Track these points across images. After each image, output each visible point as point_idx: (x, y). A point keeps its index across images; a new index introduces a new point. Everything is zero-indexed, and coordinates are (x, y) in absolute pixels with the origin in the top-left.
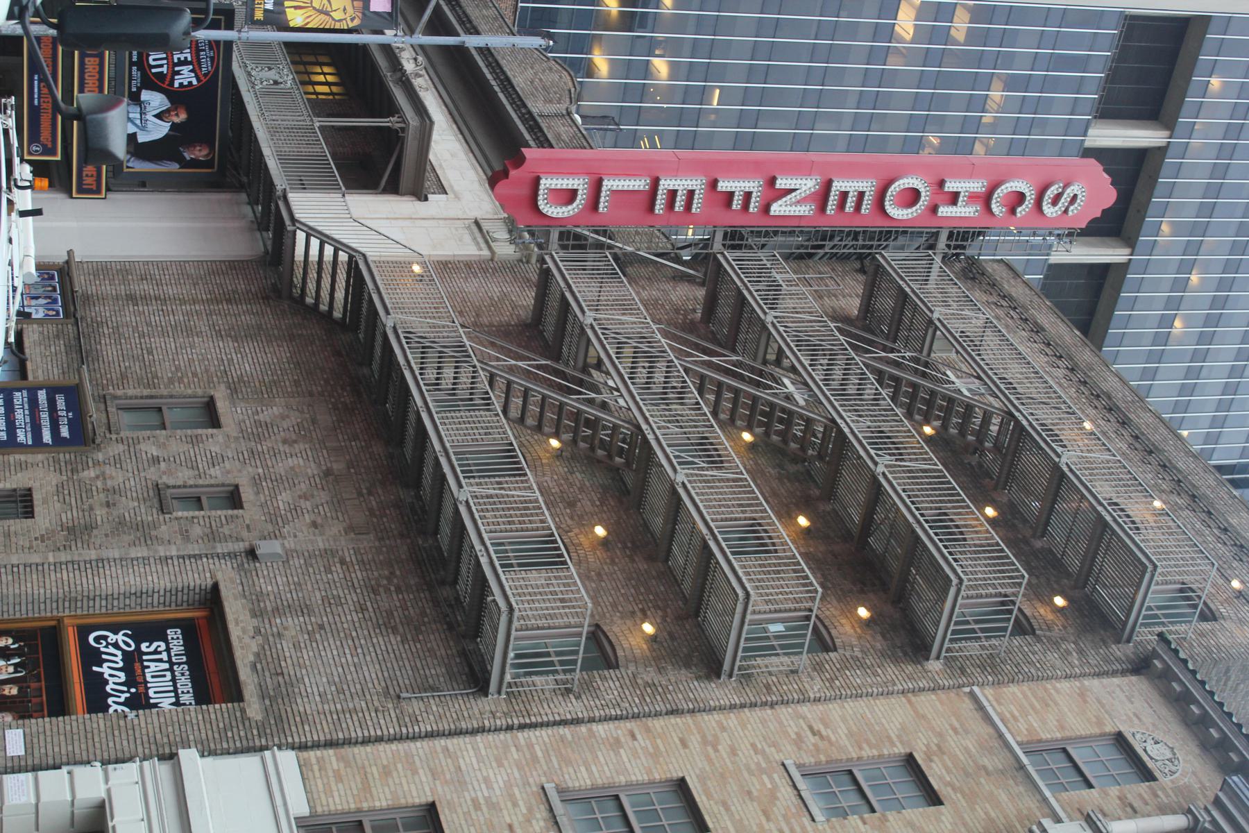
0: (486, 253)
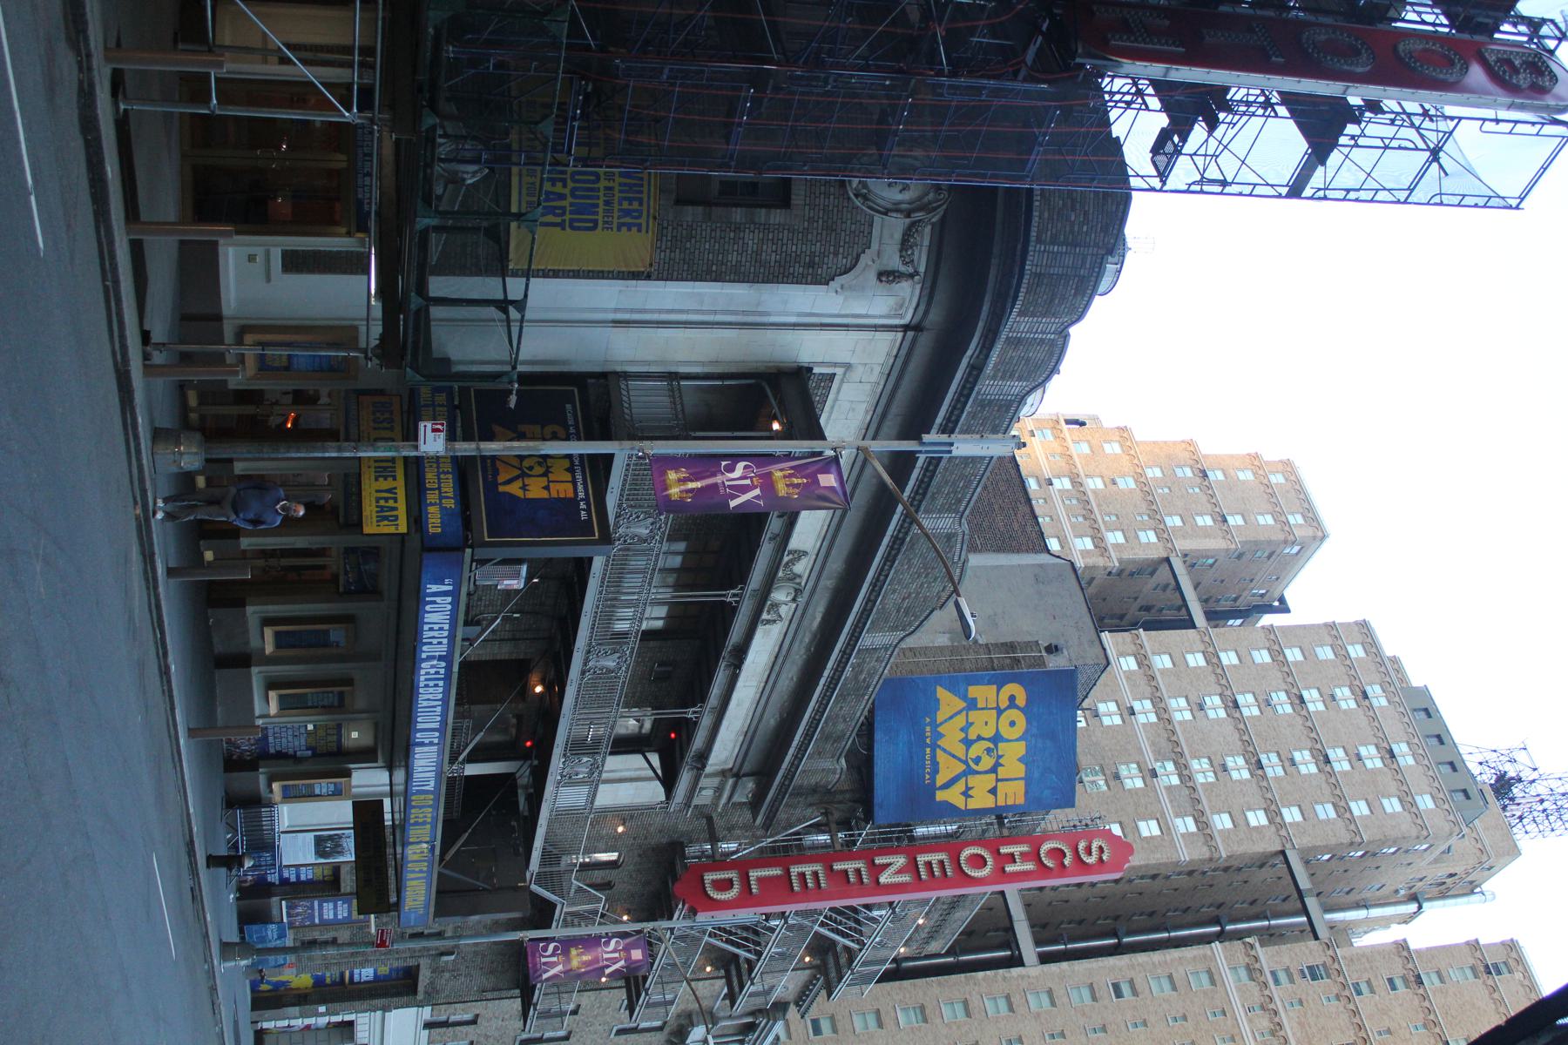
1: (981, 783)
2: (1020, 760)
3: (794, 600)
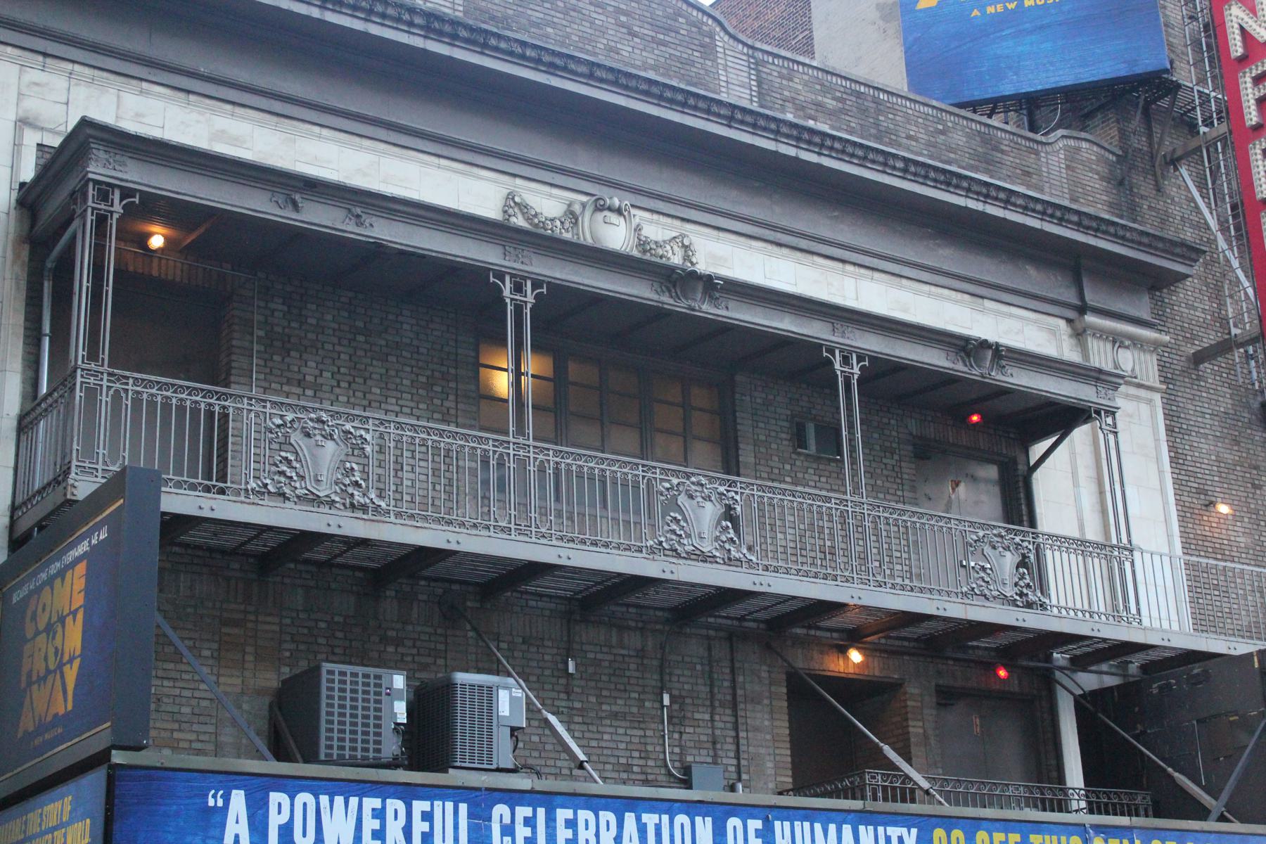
0: (1157, 397)
3: (619, 211)
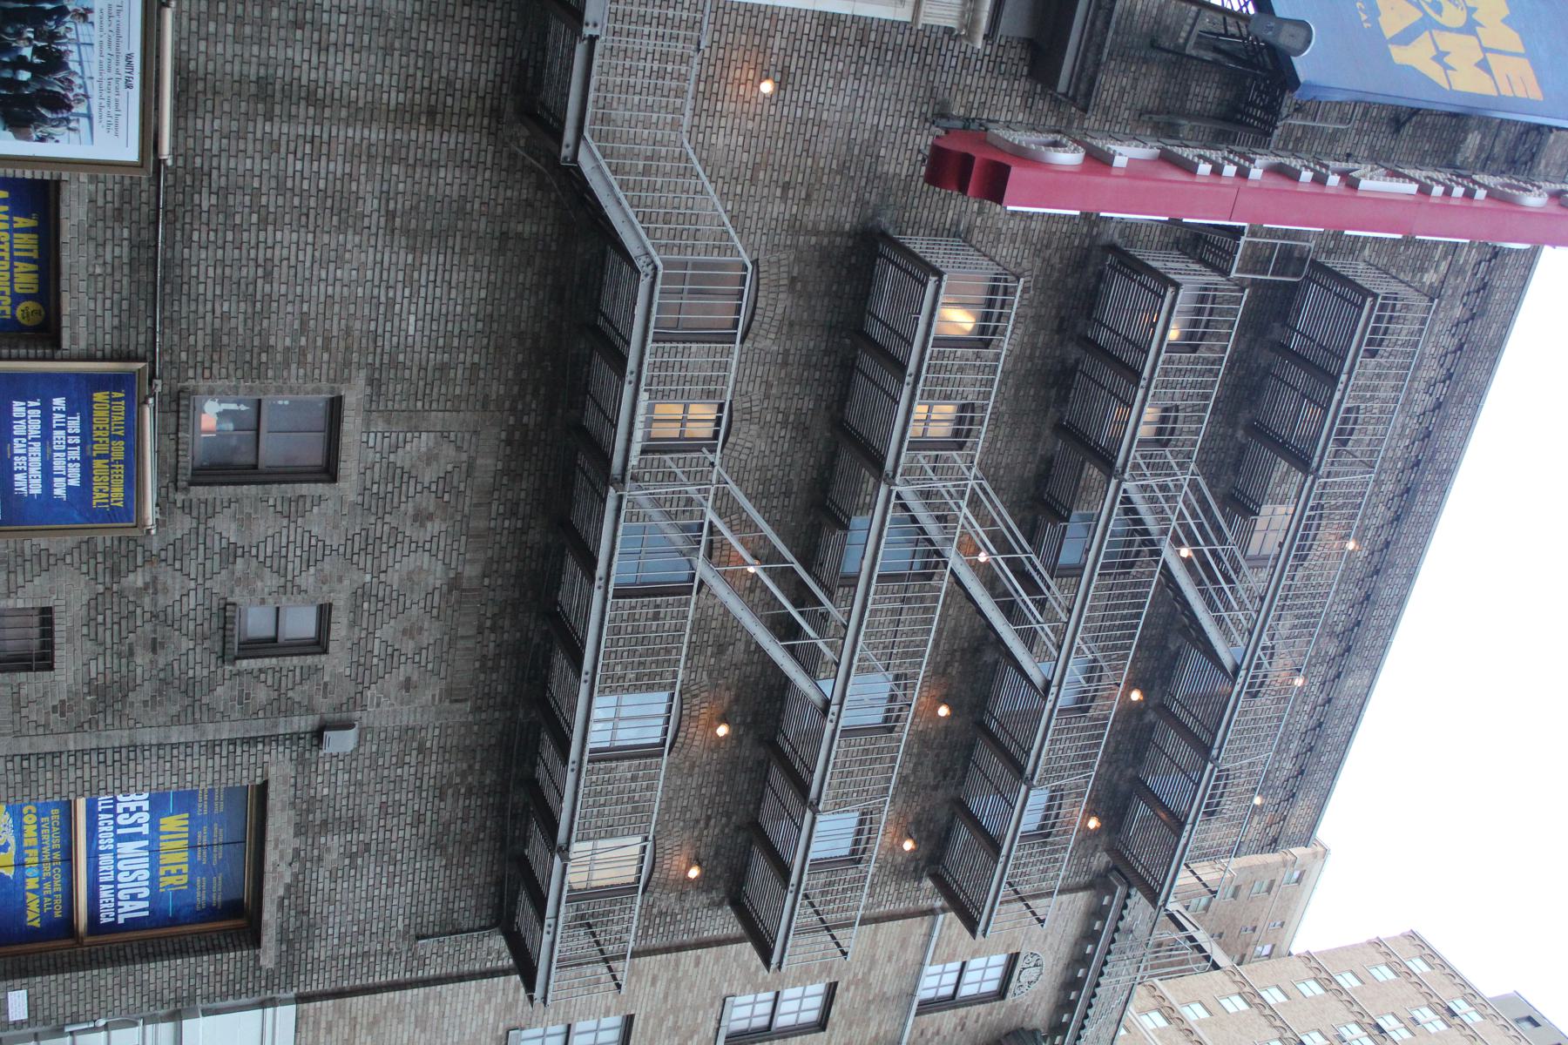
1: (1462, 51)
2: (1504, 21)
